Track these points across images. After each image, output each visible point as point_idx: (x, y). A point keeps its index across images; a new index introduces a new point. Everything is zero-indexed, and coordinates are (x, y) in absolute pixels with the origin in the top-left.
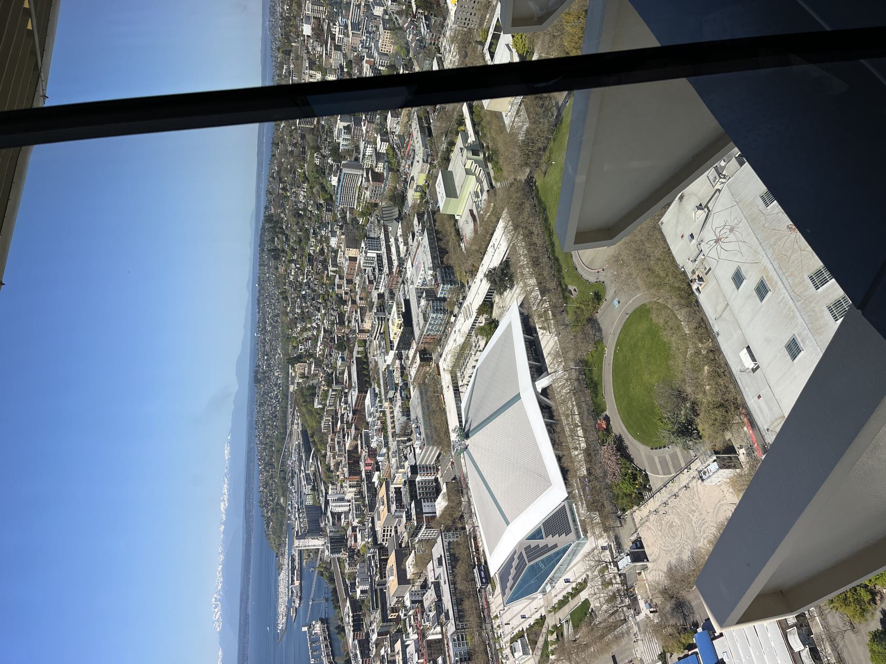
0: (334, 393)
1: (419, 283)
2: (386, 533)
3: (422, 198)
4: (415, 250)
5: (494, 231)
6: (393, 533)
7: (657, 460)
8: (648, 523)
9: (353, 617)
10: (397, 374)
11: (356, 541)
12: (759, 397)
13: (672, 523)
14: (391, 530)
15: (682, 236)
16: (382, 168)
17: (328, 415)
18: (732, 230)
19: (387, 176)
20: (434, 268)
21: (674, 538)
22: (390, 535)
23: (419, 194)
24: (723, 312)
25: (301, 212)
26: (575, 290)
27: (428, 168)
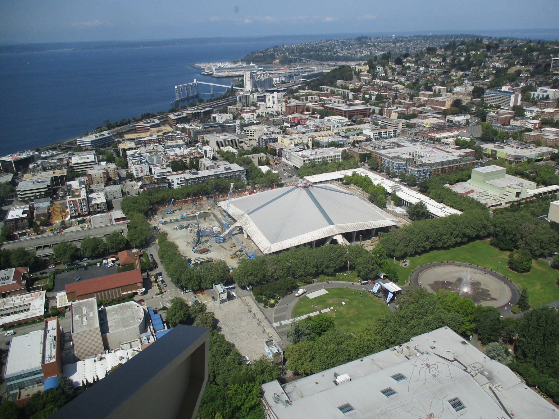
0: (346, 94)
1: (421, 153)
2: (250, 132)
3: (486, 155)
4: (447, 150)
5: (455, 208)
6: (250, 138)
7: (284, 313)
8: (243, 305)
9: (201, 112)
10: (356, 138)
11: (247, 112)
12: (317, 383)
14: (251, 136)
15: (435, 342)
16: (513, 124)
17: (331, 91)
18: (434, 376)
19: (506, 128)
20: (431, 165)
21: (234, 321)
22: (249, 136)
23: (490, 153)
24: (378, 366)
25: (483, 64)
26: (406, 265)
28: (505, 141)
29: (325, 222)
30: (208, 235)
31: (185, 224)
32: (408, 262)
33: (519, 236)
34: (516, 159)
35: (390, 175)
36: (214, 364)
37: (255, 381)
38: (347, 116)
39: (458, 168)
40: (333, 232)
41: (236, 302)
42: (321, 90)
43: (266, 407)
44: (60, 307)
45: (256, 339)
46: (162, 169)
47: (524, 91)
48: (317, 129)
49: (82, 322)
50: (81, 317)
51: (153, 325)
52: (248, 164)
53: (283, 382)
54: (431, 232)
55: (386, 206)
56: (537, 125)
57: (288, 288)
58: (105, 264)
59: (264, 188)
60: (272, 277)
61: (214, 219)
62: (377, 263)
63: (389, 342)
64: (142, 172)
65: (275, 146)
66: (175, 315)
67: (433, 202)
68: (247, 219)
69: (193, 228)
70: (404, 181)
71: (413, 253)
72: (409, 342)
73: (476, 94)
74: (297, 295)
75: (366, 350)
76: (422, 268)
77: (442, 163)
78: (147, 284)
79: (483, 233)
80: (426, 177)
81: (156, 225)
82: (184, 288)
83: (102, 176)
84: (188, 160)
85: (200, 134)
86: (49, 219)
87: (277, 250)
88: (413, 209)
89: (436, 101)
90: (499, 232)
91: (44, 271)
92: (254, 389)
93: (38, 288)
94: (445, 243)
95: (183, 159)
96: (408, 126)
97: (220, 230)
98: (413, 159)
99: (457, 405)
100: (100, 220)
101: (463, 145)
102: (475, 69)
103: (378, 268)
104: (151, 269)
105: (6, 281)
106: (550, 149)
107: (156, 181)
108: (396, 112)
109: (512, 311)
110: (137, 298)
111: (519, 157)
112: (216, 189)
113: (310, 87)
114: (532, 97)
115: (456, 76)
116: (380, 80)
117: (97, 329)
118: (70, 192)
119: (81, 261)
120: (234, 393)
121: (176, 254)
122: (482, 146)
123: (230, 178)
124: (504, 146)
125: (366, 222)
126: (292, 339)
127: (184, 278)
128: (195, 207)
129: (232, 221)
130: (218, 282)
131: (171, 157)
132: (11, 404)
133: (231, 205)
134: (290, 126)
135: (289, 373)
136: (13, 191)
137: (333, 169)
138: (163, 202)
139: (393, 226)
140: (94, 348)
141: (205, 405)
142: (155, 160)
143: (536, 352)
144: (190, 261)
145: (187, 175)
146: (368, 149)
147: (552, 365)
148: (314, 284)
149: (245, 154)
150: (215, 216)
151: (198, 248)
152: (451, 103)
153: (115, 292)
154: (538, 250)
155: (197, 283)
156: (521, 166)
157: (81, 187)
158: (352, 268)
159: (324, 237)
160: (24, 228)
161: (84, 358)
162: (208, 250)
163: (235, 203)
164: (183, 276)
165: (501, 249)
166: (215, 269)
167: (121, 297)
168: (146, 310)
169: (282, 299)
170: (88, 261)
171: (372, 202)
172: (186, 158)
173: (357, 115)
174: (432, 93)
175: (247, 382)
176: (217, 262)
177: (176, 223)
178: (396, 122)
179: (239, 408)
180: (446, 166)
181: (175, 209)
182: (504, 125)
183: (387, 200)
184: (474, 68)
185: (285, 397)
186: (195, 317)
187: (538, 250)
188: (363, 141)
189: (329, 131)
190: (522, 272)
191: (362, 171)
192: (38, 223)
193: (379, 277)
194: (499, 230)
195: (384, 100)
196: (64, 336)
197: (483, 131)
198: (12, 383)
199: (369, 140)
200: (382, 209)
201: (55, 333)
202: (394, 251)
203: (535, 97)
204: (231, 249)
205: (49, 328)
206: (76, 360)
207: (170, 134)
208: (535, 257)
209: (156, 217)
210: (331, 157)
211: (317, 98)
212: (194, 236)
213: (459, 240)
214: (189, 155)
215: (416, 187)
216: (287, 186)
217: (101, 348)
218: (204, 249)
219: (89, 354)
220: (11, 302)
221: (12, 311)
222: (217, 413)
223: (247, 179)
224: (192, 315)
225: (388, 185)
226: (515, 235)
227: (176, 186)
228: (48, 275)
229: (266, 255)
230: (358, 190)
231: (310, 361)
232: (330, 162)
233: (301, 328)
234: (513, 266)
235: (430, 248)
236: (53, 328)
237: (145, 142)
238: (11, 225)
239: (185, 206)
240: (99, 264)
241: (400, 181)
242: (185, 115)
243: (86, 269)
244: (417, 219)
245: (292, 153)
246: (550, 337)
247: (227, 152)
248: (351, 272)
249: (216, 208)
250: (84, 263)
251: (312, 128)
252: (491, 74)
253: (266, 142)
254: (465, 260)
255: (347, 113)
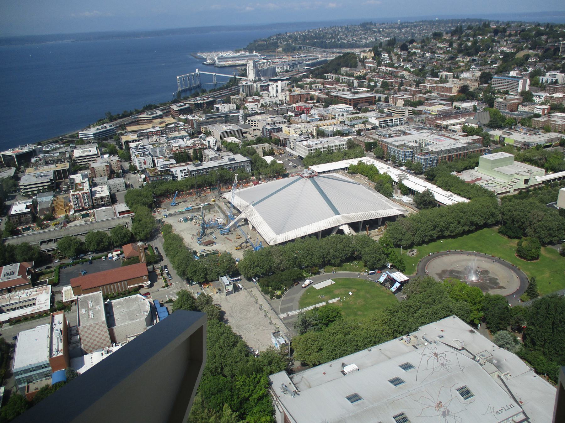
0: (351, 81)
2: (253, 122)
3: (494, 142)
4: (454, 137)
5: (462, 197)
6: (254, 128)
7: (291, 304)
8: (249, 296)
9: (203, 103)
10: (361, 126)
11: (250, 102)
12: (324, 374)
13: (249, 312)
14: (256, 126)
15: (443, 331)
16: (521, 110)
17: (336, 78)
18: (442, 365)
19: (514, 114)
20: (438, 153)
22: (252, 126)
23: (498, 139)
24: (386, 355)
26: (413, 254)
27: (518, 146)
28: (513, 127)
29: (331, 211)
30: (213, 227)
31: (189, 216)
32: (415, 251)
33: (527, 223)
34: (524, 145)
35: (397, 164)
36: (221, 356)
37: (262, 372)
38: (352, 104)
39: (465, 155)
40: (339, 222)
41: (242, 294)
42: (325, 78)
43: (274, 397)
44: (66, 301)
45: (263, 330)
46: (166, 161)
47: (532, 76)
48: (322, 118)
49: (89, 316)
50: (87, 311)
51: (159, 318)
52: (252, 155)
53: (290, 372)
54: (439, 220)
55: (392, 195)
56: (546, 110)
57: (294, 279)
58: (110, 258)
59: (269, 178)
60: (278, 268)
61: (219, 211)
62: (384, 253)
63: (397, 331)
64: (145, 164)
65: (279, 136)
66: (181, 307)
67: (440, 190)
68: (252, 210)
69: (198, 220)
70: (411, 170)
71: (421, 242)
72: (417, 332)
73: (483, 79)
74: (303, 285)
75: (374, 340)
76: (430, 257)
77: (449, 151)
78: (153, 277)
79: (491, 221)
80: (432, 165)
81: (160, 218)
82: (189, 281)
83: (105, 169)
84: (191, 152)
85: (203, 125)
86: (53, 213)
87: (282, 241)
88: (420, 198)
89: (443, 87)
90: (507, 220)
91: (49, 265)
92: (262, 380)
93: (44, 283)
94: (453, 232)
95: (187, 151)
96: (414, 113)
97: (224, 221)
98: (420, 147)
99: (466, 393)
100: (104, 214)
101: (470, 132)
102: (483, 54)
103: (385, 257)
104: (156, 262)
105: (12, 276)
106: (559, 135)
107: (159, 173)
108: (402, 99)
109: (520, 299)
110: (143, 291)
111: (527, 144)
112: (220, 180)
113: (314, 75)
114: (541, 82)
115: (463, 62)
116: (386, 67)
117: (103, 322)
118: (73, 185)
119: (85, 255)
120: (242, 384)
121: (181, 247)
122: (490, 133)
123: (234, 169)
124: (513, 133)
125: (373, 212)
126: (299, 329)
127: (189, 271)
128: (199, 199)
129: (237, 212)
130: (223, 274)
131: (174, 149)
132: (21, 398)
133: (236, 197)
134: (294, 116)
135: (297, 364)
136: (16, 185)
137: (338, 159)
138: (167, 194)
139: (400, 215)
140: (101, 341)
141: (213, 397)
142: (158, 152)
143: (545, 340)
144: (195, 253)
145: (191, 167)
146: (374, 137)
147: (561, 353)
148: (321, 275)
149: (249, 145)
150: (219, 207)
151: (203, 240)
152: (458, 89)
153: (121, 285)
154: (546, 237)
155: (202, 275)
156: (529, 152)
157: (84, 181)
158: (359, 258)
159: (330, 227)
160: (27, 223)
161: (91, 352)
162: (214, 242)
163: (239, 195)
164: (189, 268)
165: (510, 237)
166: (221, 261)
167: (127, 291)
168: (152, 302)
169: (288, 291)
170: (92, 255)
171: (379, 191)
172: (190, 149)
173: (362, 103)
174: (439, 79)
175: (254, 374)
176: (223, 254)
177: (180, 215)
178: (402, 109)
179: (247, 399)
180: (453, 154)
181: (179, 202)
182: (512, 111)
183: (394, 188)
184: (481, 53)
185: (293, 388)
186: (202, 309)
187: (546, 237)
188: (368, 129)
189: (334, 120)
190: (531, 260)
191: (368, 160)
192: (42, 217)
193: (387, 267)
194: (508, 217)
195: (390, 87)
196: (71, 330)
197: (491, 117)
198: (20, 377)
199: (375, 128)
200: (389, 198)
201: (61, 327)
202: (401, 240)
203: (544, 81)
204: (236, 240)
205: (56, 322)
206: (83, 353)
207: (173, 125)
208: (544, 244)
209: (160, 209)
210: (336, 146)
211: (321, 87)
212: (199, 228)
213: (467, 228)
214: (192, 147)
215: (423, 176)
216: (292, 176)
217: (108, 342)
218: (209, 241)
219: (96, 347)
220: (17, 297)
221: (18, 305)
222: (225, 404)
223: (252, 170)
224: (198, 307)
225: (394, 173)
226: (523, 223)
227: (179, 178)
228: (53, 269)
229: (272, 246)
230: (364, 179)
231: (318, 352)
232: (335, 151)
233: (308, 319)
234: (522, 254)
235: (437, 237)
236: (59, 322)
237: (148, 134)
238: (15, 220)
239: (189, 198)
240: (103, 257)
241: (407, 169)
242: (187, 106)
243: (91, 263)
244: (425, 208)
245: (297, 143)
246: (560, 325)
247: (231, 143)
248: (358, 262)
249: (221, 200)
250: (89, 257)
251: (317, 117)
252: (498, 59)
253: (271, 132)
254: (473, 248)
255: (352, 101)
